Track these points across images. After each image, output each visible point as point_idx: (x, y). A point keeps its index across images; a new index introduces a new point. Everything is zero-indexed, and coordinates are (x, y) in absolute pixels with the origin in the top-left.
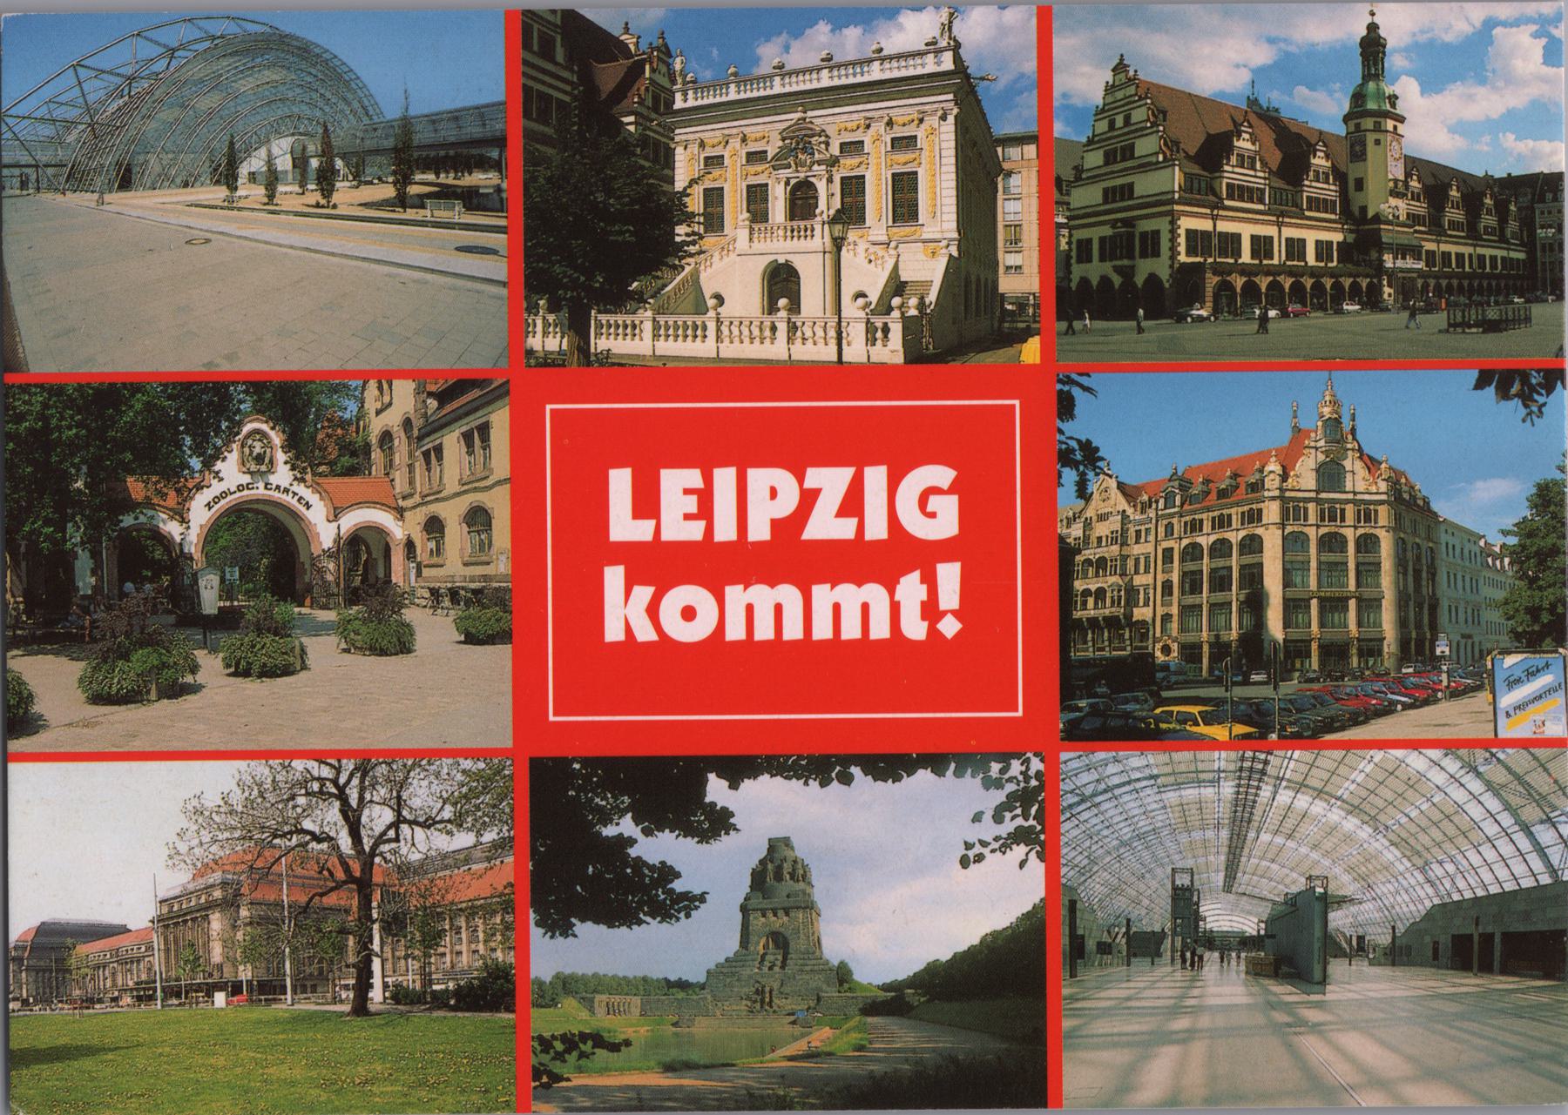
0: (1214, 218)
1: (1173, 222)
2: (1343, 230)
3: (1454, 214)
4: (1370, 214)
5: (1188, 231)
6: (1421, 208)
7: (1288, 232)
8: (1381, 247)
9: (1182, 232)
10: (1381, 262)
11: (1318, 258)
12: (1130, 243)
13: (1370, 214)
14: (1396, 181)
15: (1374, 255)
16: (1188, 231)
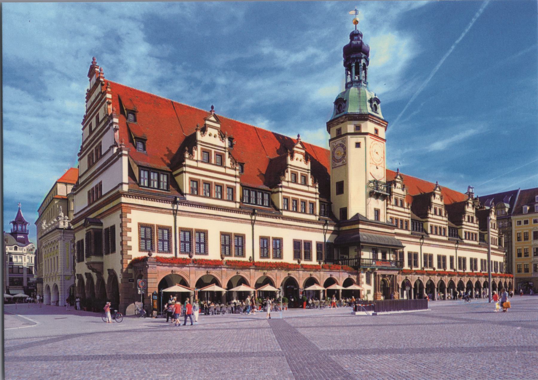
0: (175, 213)
1: (121, 217)
2: (325, 232)
3: (437, 220)
4: (351, 214)
5: (141, 226)
6: (405, 213)
7: (262, 231)
8: (359, 245)
9: (133, 226)
10: (359, 258)
11: (297, 255)
12: (102, 240)
13: (351, 214)
14: (376, 182)
15: (352, 254)
16: (141, 226)
